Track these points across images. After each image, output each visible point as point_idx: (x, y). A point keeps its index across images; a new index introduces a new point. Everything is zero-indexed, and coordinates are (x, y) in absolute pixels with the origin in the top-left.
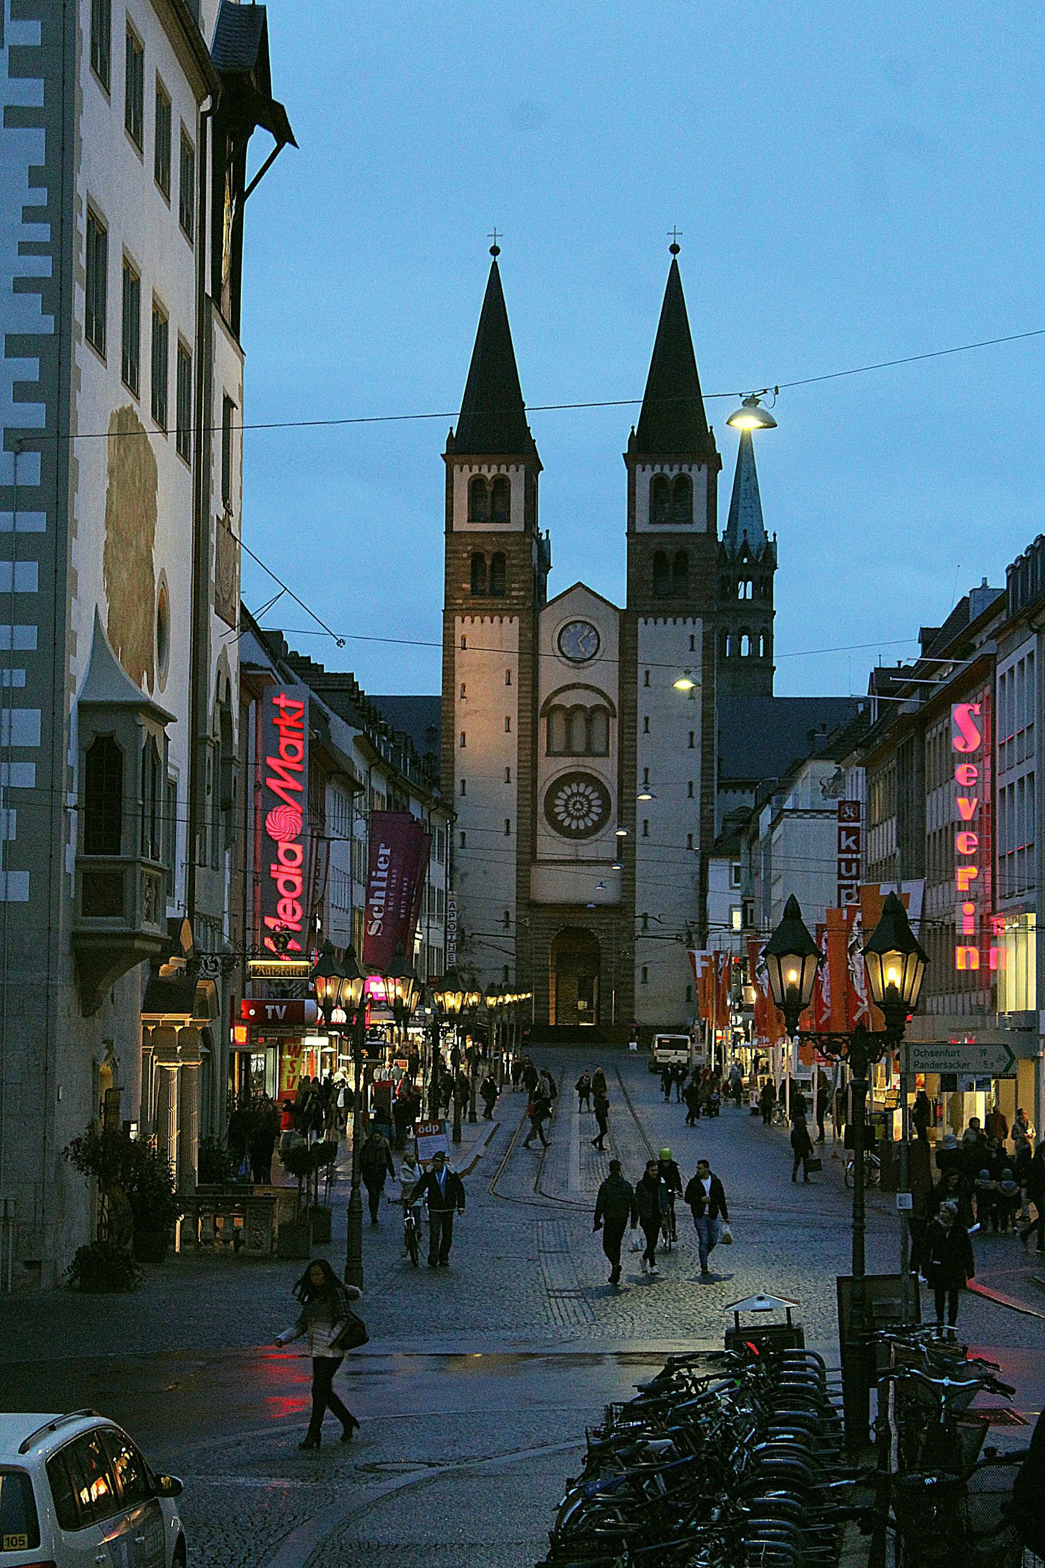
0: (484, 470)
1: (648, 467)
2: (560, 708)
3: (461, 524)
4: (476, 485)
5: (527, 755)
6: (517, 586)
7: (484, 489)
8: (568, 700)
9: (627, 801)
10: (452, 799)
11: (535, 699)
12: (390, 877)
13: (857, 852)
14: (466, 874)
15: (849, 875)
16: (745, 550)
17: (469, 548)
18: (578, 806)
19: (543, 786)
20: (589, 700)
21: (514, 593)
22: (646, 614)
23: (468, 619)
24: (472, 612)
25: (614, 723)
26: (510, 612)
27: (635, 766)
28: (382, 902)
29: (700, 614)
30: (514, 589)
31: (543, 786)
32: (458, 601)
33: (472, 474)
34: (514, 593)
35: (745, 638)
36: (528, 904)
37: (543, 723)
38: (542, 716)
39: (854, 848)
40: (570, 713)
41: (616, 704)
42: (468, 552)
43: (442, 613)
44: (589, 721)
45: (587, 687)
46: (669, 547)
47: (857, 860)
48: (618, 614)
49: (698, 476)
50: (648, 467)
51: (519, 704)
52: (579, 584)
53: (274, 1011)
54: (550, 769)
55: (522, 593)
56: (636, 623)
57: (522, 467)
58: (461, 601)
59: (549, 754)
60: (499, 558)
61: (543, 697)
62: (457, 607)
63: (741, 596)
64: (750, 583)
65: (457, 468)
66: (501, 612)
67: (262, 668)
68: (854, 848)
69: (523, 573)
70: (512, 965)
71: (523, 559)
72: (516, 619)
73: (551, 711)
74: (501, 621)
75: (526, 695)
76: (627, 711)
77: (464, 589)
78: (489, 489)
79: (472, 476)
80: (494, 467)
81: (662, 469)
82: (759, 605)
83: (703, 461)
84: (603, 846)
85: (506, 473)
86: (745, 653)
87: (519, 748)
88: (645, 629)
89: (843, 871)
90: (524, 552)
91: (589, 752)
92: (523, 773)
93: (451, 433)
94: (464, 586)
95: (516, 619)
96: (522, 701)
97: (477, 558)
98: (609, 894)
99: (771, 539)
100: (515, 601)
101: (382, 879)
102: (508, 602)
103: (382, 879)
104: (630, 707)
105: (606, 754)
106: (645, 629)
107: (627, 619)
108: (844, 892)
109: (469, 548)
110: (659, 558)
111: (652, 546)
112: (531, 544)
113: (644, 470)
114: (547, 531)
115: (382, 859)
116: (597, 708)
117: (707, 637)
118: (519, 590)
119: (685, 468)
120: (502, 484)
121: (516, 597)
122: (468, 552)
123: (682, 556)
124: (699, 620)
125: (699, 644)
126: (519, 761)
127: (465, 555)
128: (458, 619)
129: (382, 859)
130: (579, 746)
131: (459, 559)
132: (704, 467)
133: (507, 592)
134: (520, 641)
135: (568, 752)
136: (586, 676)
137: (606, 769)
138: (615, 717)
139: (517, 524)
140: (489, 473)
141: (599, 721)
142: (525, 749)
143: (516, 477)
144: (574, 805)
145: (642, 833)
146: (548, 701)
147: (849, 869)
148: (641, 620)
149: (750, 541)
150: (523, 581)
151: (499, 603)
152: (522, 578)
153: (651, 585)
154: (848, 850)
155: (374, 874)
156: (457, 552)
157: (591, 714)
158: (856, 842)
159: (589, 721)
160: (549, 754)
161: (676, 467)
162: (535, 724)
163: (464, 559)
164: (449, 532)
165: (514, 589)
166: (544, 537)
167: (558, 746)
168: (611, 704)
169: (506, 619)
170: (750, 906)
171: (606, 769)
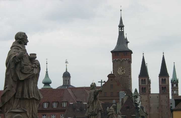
49: (167, 79)
60: (145, 88)
82: (176, 87)
86: (175, 93)
88: (161, 96)
120: (145, 80)
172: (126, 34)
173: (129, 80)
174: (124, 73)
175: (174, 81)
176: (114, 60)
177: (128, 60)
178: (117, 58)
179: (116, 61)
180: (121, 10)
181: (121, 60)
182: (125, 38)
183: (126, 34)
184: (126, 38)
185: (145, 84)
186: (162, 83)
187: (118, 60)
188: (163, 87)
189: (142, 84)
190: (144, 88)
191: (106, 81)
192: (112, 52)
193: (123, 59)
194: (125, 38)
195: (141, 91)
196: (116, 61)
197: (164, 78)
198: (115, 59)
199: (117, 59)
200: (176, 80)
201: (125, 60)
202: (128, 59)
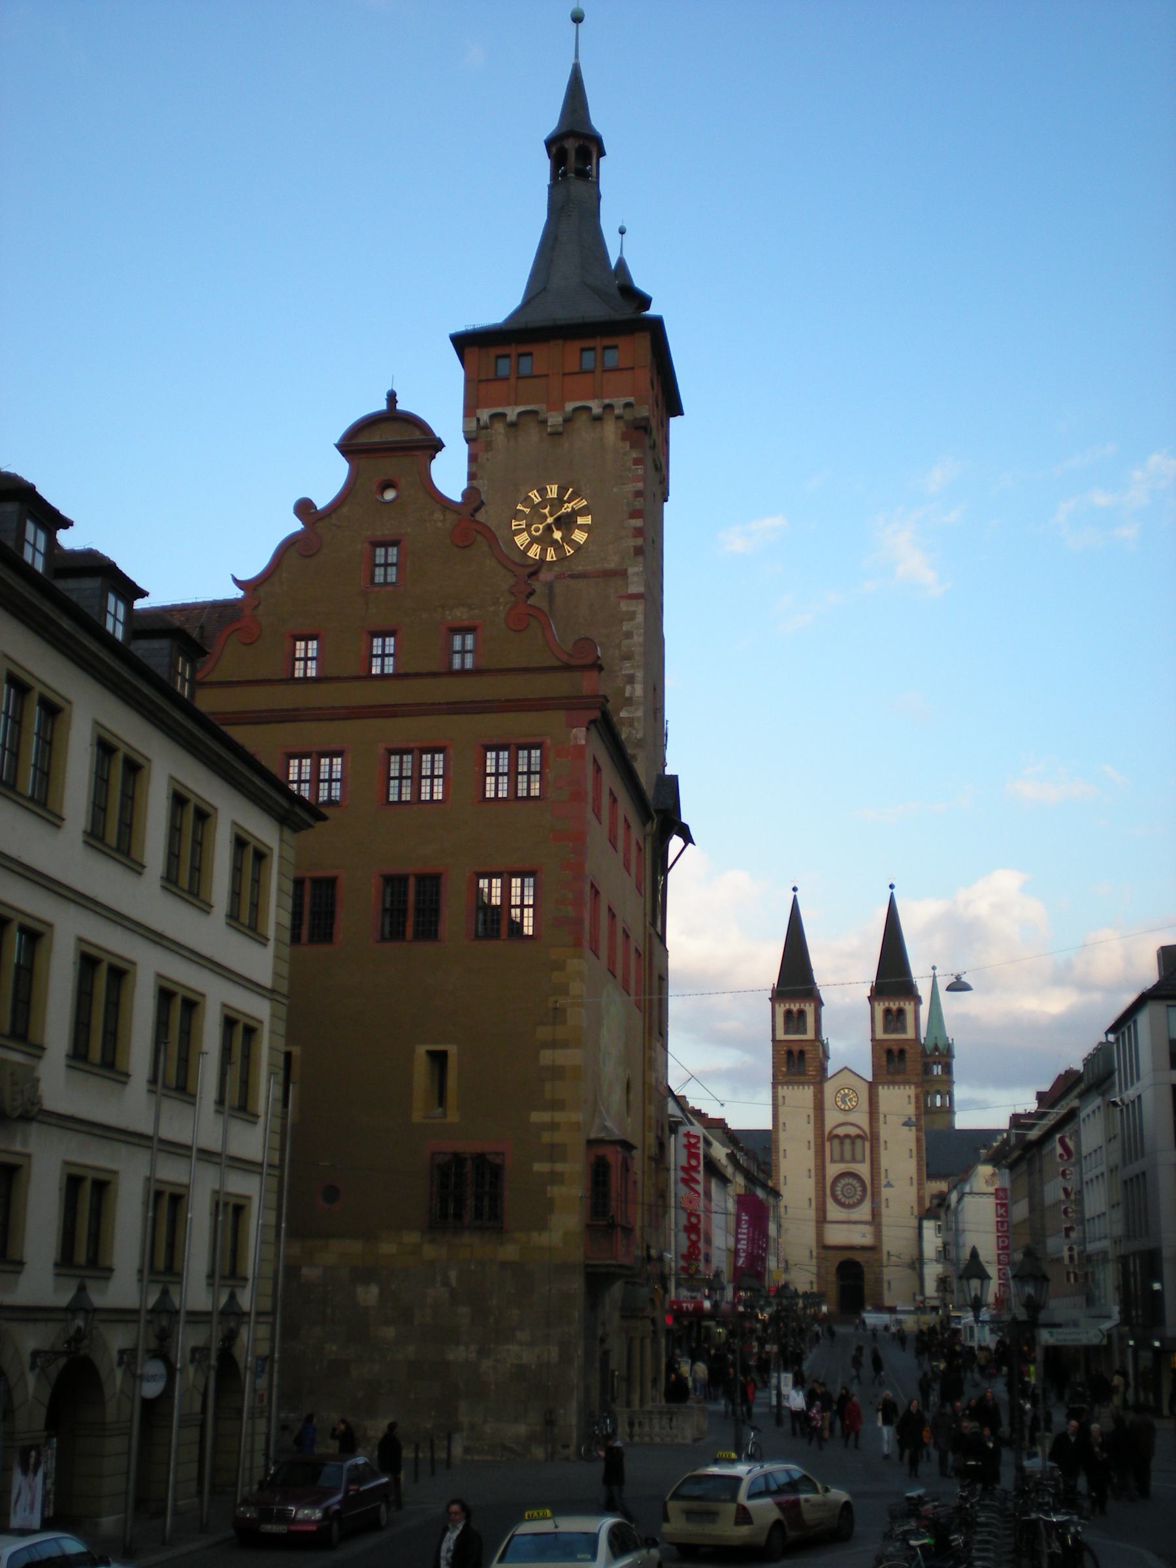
0: (792, 1007)
1: (881, 1004)
2: (837, 1136)
3: (781, 1036)
4: (788, 1013)
7: (793, 1017)
8: (841, 1131)
11: (823, 1131)
12: (749, 1231)
13: (1006, 1217)
14: (786, 1230)
15: (1003, 1230)
16: (936, 1048)
18: (849, 1191)
19: (829, 1181)
20: (853, 1131)
22: (883, 1084)
23: (785, 1087)
24: (787, 1083)
25: (867, 1145)
26: (808, 1083)
27: (880, 1168)
28: (745, 1247)
30: (811, 1071)
31: (829, 1181)
34: (810, 1073)
35: (938, 1097)
36: (824, 1247)
37: (827, 1144)
39: (1004, 1214)
40: (842, 1139)
41: (868, 1134)
42: (784, 1051)
44: (853, 1143)
45: (852, 1124)
47: (1007, 1222)
48: (867, 1084)
49: (909, 1007)
50: (881, 1004)
52: (846, 1068)
53: (687, 1307)
54: (833, 1170)
55: (814, 1073)
56: (878, 1088)
57: (813, 1005)
60: (802, 1053)
61: (828, 1128)
62: (779, 1081)
63: (935, 1073)
64: (940, 1066)
65: (777, 1006)
66: (803, 1084)
67: (677, 1117)
68: (1004, 1214)
70: (815, 1280)
73: (833, 1137)
74: (804, 1088)
76: (873, 1138)
78: (795, 1016)
79: (786, 1010)
80: (797, 1005)
81: (889, 1004)
82: (945, 1077)
83: (912, 1000)
84: (863, 1212)
86: (938, 1104)
88: (884, 1092)
89: (1000, 1228)
90: (815, 1050)
91: (854, 1160)
93: (774, 987)
95: (812, 1087)
97: (790, 1053)
98: (868, 1241)
99: (950, 1042)
101: (744, 1234)
102: (807, 1077)
103: (744, 1234)
105: (863, 1161)
106: (884, 1092)
107: (872, 1086)
108: (1000, 1240)
109: (785, 1048)
110: (889, 1052)
112: (819, 1046)
113: (879, 1005)
114: (827, 1039)
115: (744, 1222)
116: (858, 1136)
117: (917, 1097)
119: (902, 1004)
120: (802, 1013)
121: (812, 1075)
122: (784, 1051)
123: (902, 1052)
124: (913, 1087)
125: (913, 1100)
126: (816, 1166)
127: (783, 1052)
128: (780, 1088)
129: (744, 1222)
130: (848, 1155)
132: (912, 1003)
134: (814, 1099)
135: (842, 1160)
136: (853, 1117)
137: (863, 1169)
138: (868, 1140)
139: (810, 1035)
140: (795, 1007)
141: (859, 1142)
143: (809, 1009)
144: (847, 1190)
146: (830, 1132)
147: (1002, 1226)
148: (880, 1087)
149: (939, 1044)
150: (815, 1067)
151: (802, 1078)
152: (815, 1064)
153: (886, 1068)
154: (1001, 1216)
155: (740, 1231)
156: (778, 1051)
157: (853, 1139)
158: (1006, 1211)
159: (853, 1143)
160: (832, 1161)
161: (897, 1003)
162: (823, 1145)
163: (783, 1054)
164: (774, 1040)
166: (825, 1042)
167: (837, 1156)
168: (866, 1134)
169: (806, 1087)
170: (947, 1247)
171: (863, 1169)
172: (622, 232)
173: (625, 606)
174: (580, 537)
175: (936, 1048)
176: (484, 415)
177: (619, 418)
178: (509, 404)
179: (499, 427)
180: (577, 19)
181: (555, 419)
182: (613, 262)
183: (622, 232)
184: (621, 263)
185: (805, 1032)
186: (886, 1030)
187: (520, 414)
188: (889, 1052)
189: (786, 1032)
190: (796, 1054)
191: (321, 503)
192: (464, 343)
193: (570, 406)
194: (613, 262)
195: (784, 1069)
196: (499, 427)
197: (894, 1006)
198: (499, 410)
199: (512, 413)
200: (941, 1046)
201: (598, 419)
202: (628, 405)
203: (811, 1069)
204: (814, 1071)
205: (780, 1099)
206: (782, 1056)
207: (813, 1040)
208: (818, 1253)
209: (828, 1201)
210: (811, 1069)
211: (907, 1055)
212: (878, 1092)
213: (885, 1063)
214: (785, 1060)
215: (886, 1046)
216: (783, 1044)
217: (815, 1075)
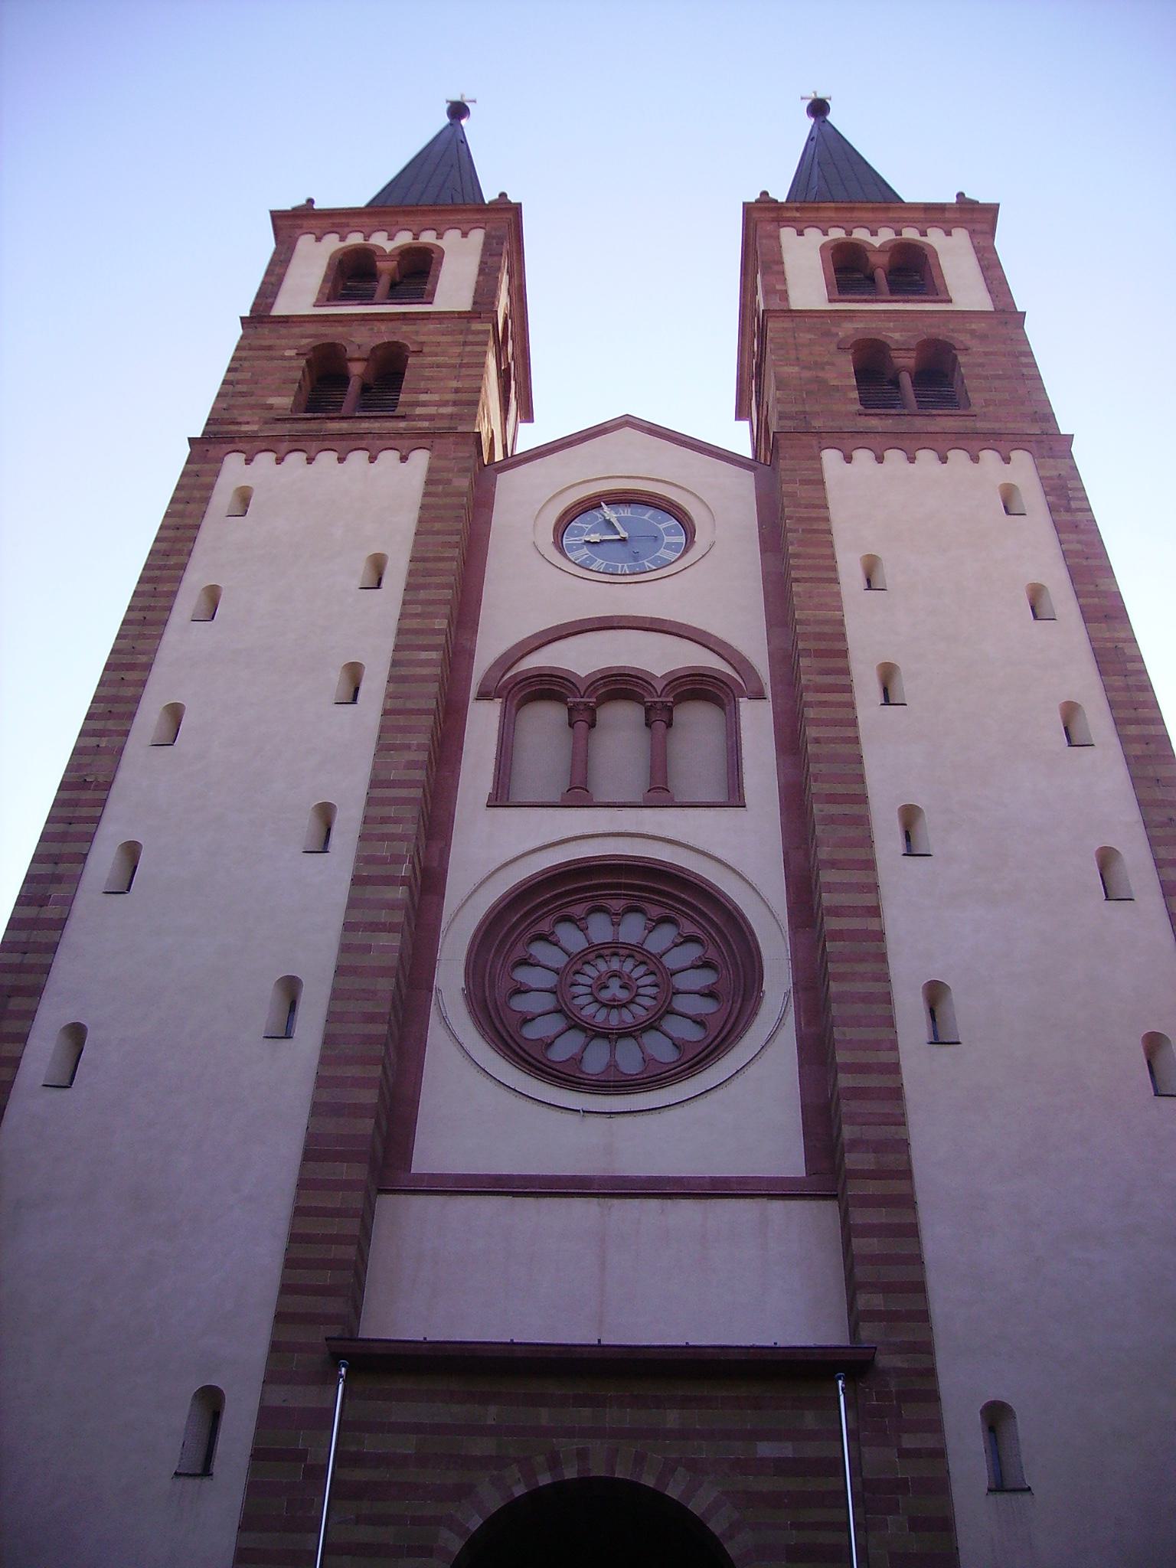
5: (411, 765)
6: (436, 397)
9: (837, 912)
10: (68, 902)
17: (304, 341)
18: (615, 990)
21: (419, 411)
26: (405, 444)
29: (1020, 440)
30: (424, 404)
32: (244, 428)
33: (342, 245)
34: (419, 411)
38: (484, 695)
43: (186, 450)
46: (897, 336)
51: (400, 632)
57: (477, 236)
58: (255, 428)
59: (500, 798)
69: (457, 378)
71: (460, 355)
72: (420, 460)
75: (431, 609)
77: (271, 407)
83: (958, 223)
85: (439, 243)
87: (383, 747)
92: (385, 820)
94: (272, 401)
96: (414, 624)
100: (426, 424)
102: (403, 424)
104: (820, 637)
109: (304, 341)
111: (841, 334)
118: (444, 403)
125: (1033, 497)
126: (375, 783)
131: (272, 358)
133: (400, 411)
138: (759, 696)
142: (408, 747)
145: (924, 1032)
148: (831, 458)
150: (457, 391)
152: (454, 384)
153: (855, 395)
156: (270, 348)
160: (500, 798)
163: (290, 358)
164: (259, 319)
165: (424, 404)
169: (389, 458)
195: (283, 402)
203: (423, 397)
204: (455, 403)
205: (222, 496)
206: (286, 363)
207: (460, 315)
208: (267, 1416)
209: (435, 1034)
210: (423, 397)
211: (961, 359)
212: (820, 470)
213: (854, 382)
214: (299, 375)
215: (847, 330)
216: (297, 330)
217: (451, 416)
